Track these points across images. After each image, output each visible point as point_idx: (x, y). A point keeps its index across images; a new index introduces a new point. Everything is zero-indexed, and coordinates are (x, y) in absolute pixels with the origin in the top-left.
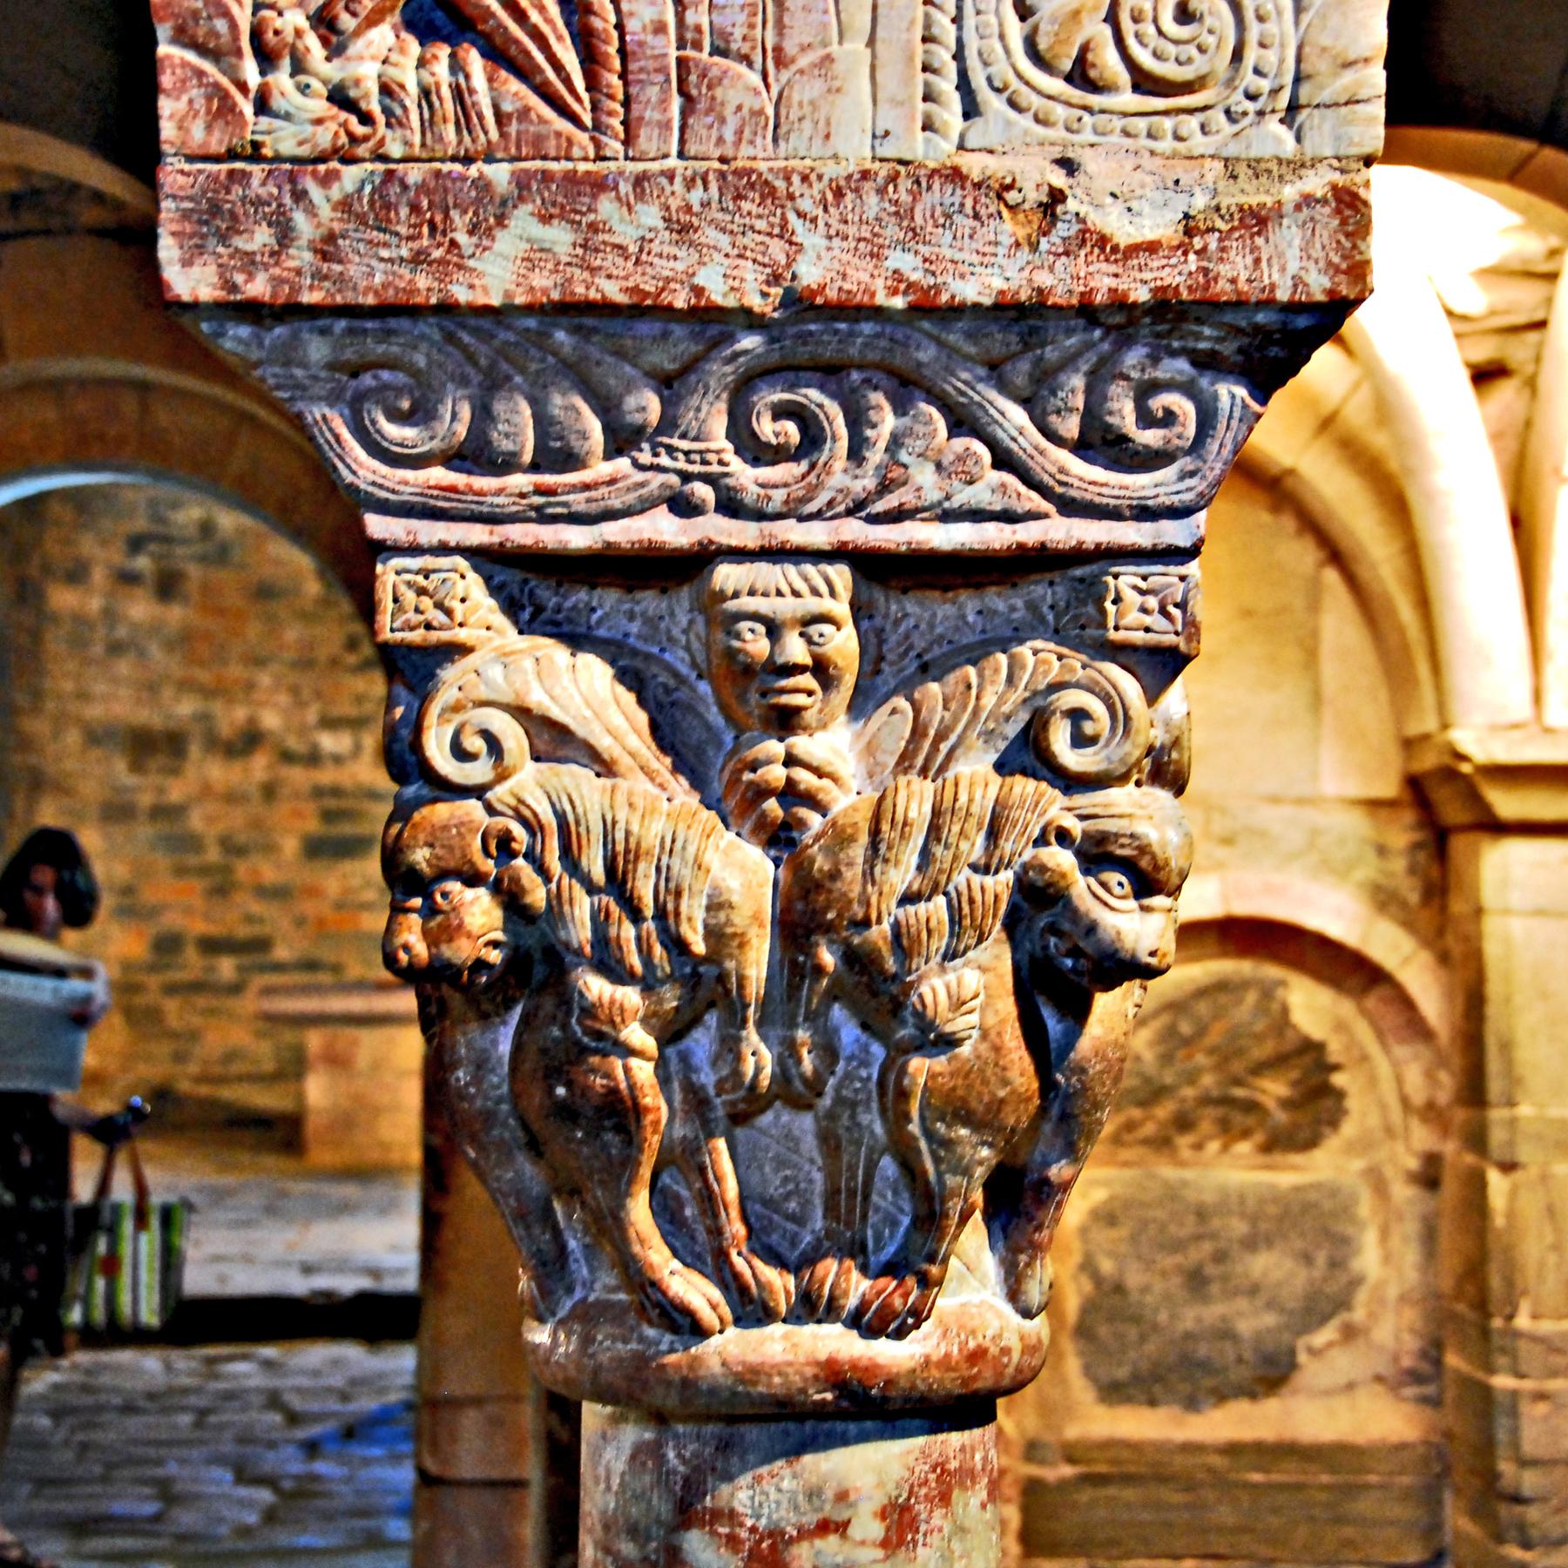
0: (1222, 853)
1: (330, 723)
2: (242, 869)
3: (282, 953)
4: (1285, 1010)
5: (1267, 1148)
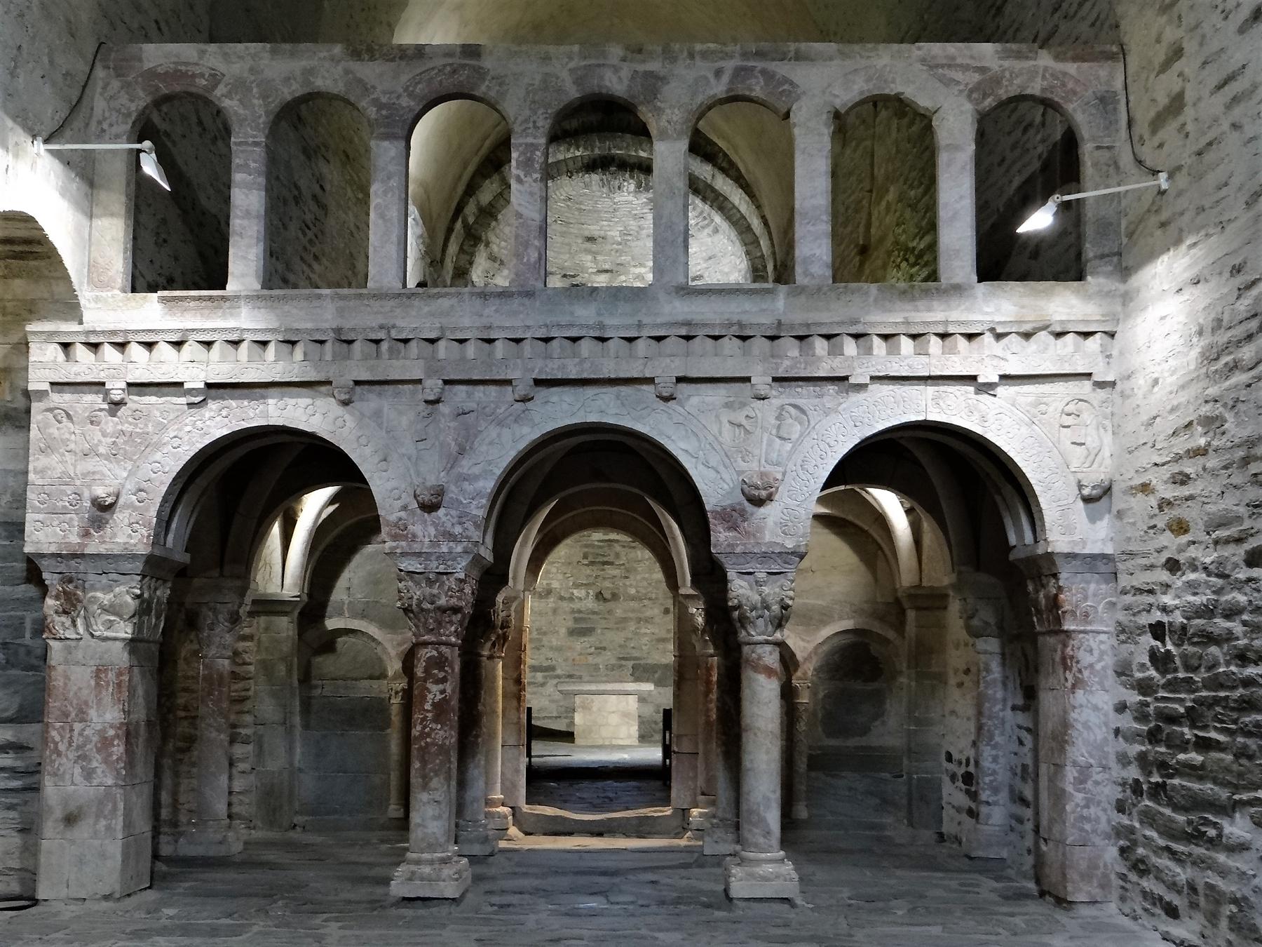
1: (576, 586)
2: (545, 640)
3: (559, 672)
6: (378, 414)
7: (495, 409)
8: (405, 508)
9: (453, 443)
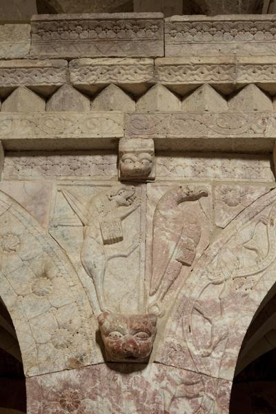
6: (39, 198)
7: (243, 195)
8: (77, 363)
9: (172, 245)
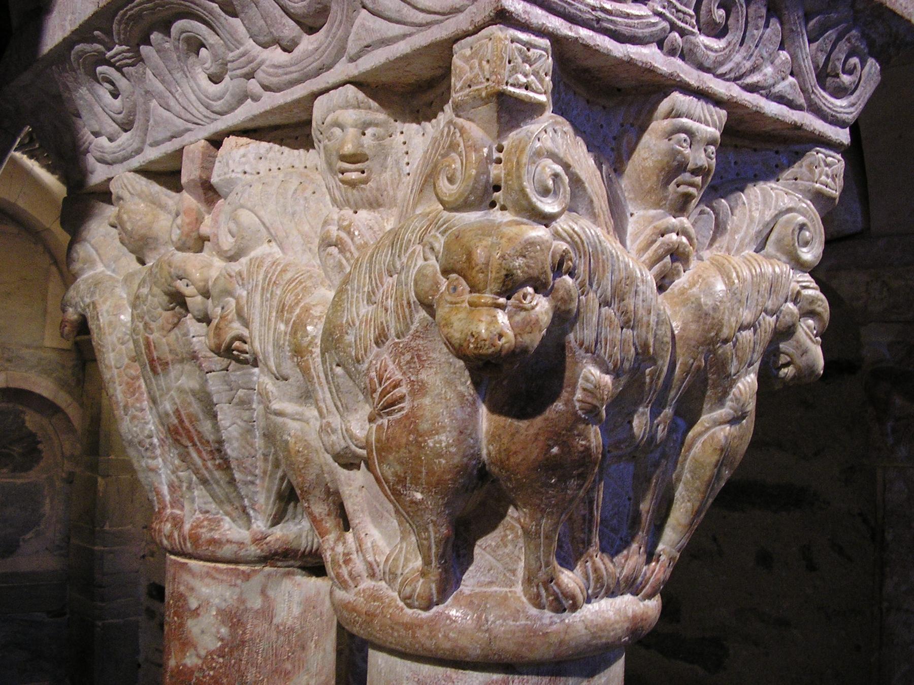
0: (7, 365)
4: (24, 422)
5: (13, 471)
